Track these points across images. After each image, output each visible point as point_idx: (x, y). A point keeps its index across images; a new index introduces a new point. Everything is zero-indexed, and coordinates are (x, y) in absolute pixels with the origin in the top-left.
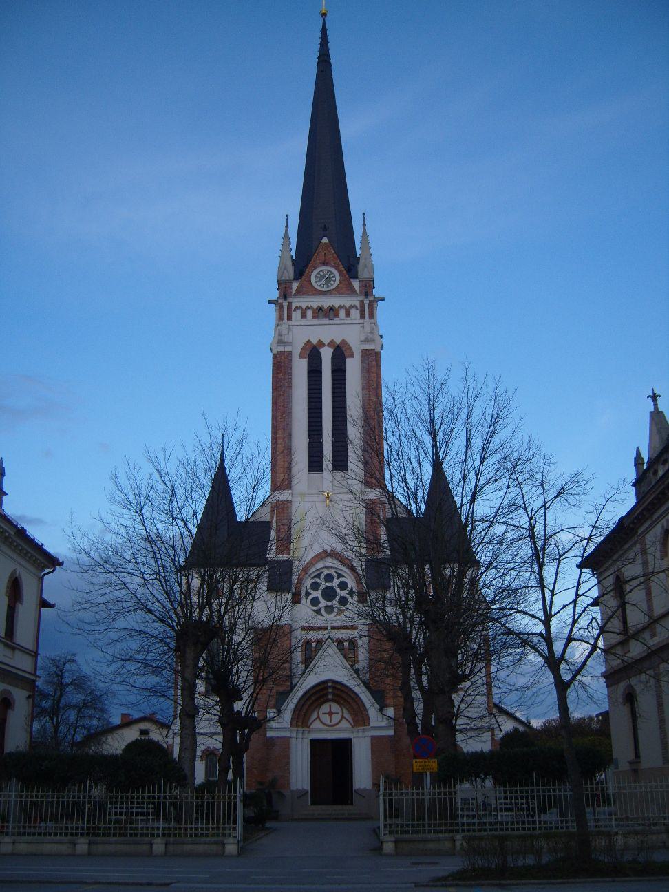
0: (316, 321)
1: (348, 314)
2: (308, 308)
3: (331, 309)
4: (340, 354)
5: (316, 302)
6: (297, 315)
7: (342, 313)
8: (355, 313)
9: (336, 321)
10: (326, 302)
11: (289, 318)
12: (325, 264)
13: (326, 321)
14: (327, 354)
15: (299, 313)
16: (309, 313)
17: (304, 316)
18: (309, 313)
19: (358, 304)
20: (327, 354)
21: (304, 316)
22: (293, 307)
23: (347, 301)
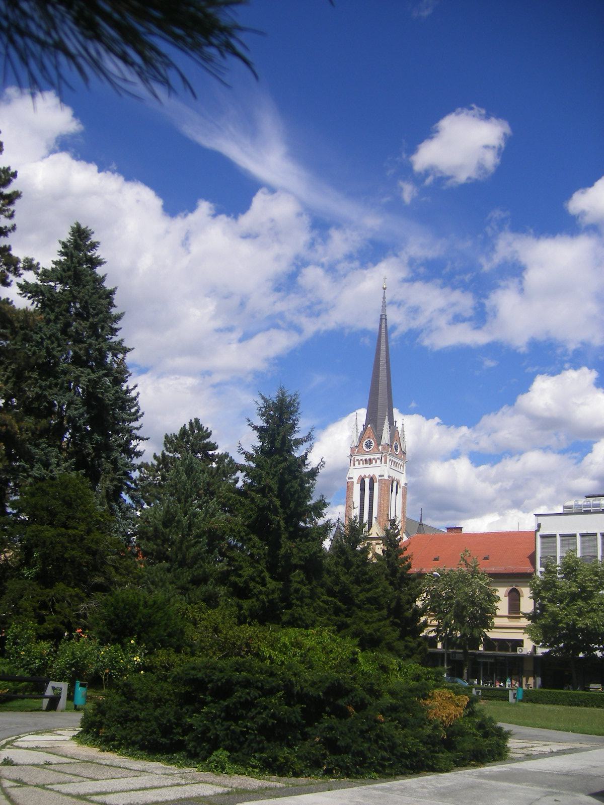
0: (365, 466)
1: (376, 462)
2: (362, 460)
3: (370, 460)
4: (372, 481)
5: (364, 458)
6: (357, 463)
7: (374, 461)
8: (378, 461)
9: (371, 465)
10: (368, 457)
11: (354, 465)
12: (369, 438)
13: (368, 465)
14: (367, 481)
15: (357, 462)
16: (361, 462)
17: (359, 464)
18: (361, 462)
19: (380, 457)
20: (367, 481)
21: (359, 464)
22: (356, 459)
23: (376, 456)
